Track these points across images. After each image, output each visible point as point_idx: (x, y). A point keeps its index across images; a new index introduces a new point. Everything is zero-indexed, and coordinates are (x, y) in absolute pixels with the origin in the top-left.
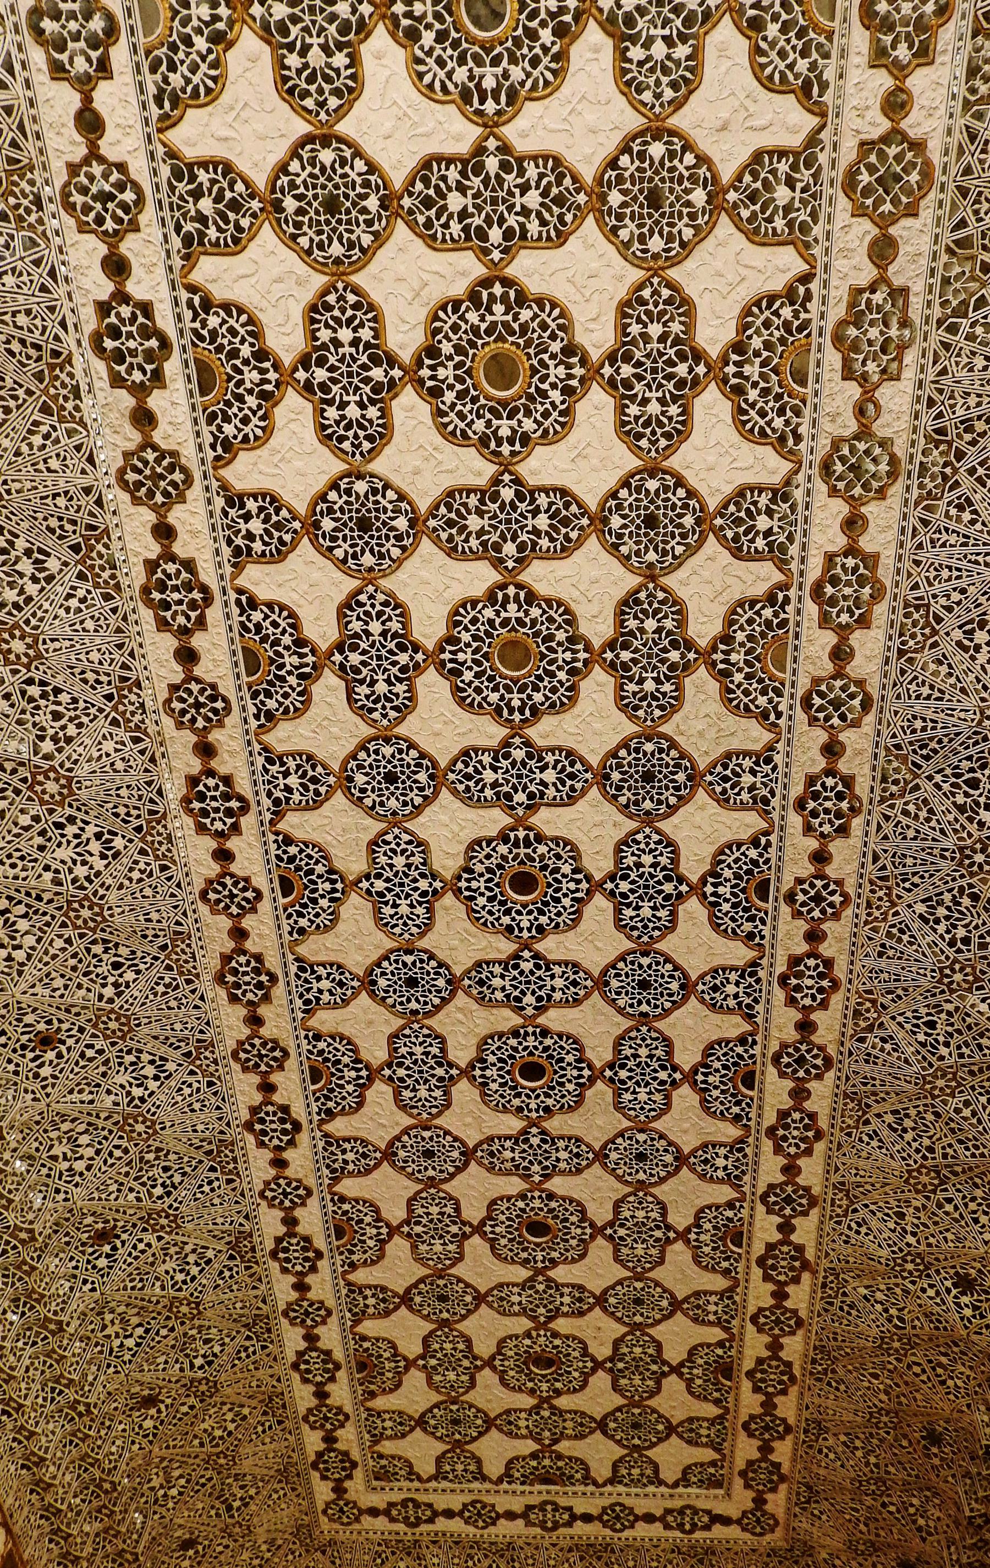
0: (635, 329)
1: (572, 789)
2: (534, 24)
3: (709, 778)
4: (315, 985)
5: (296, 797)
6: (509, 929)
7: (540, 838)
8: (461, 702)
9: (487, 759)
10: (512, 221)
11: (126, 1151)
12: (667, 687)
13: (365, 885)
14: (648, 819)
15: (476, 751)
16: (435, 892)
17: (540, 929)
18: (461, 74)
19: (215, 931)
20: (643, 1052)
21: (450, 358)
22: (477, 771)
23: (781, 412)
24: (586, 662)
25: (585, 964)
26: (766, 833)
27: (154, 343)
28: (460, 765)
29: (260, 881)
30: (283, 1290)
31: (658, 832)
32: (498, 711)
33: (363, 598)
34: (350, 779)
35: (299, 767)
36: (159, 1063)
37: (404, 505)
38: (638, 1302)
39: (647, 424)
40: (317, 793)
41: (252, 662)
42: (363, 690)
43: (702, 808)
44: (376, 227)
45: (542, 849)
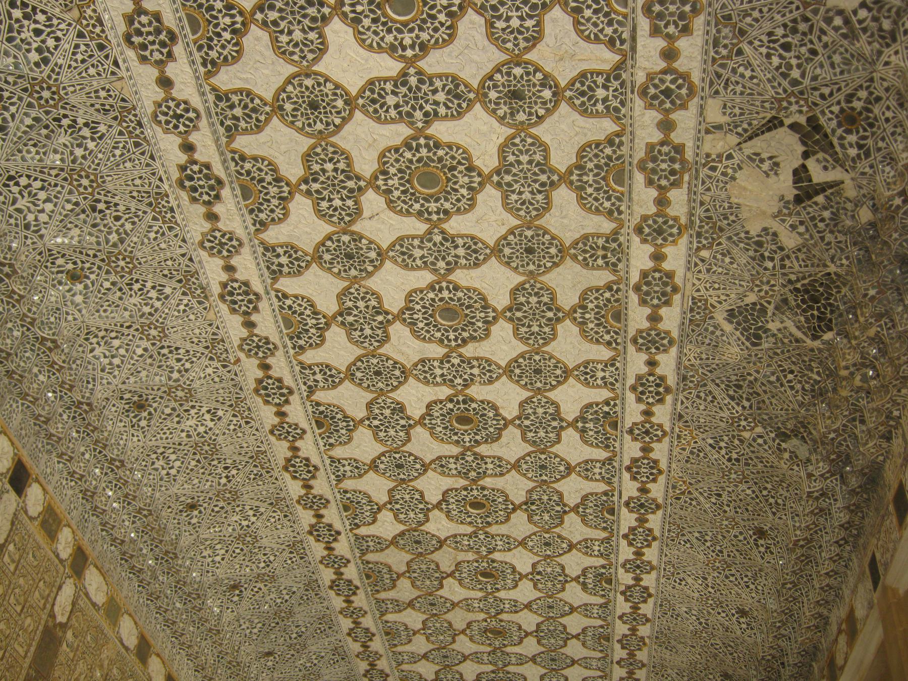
0: (511, 158)
2: (434, 12)
5: (321, 384)
9: (436, 364)
10: (428, 108)
11: (242, 550)
12: (547, 329)
16: (410, 425)
17: (476, 441)
18: (389, 38)
19: (280, 450)
20: (545, 498)
21: (395, 175)
23: (609, 199)
24: (494, 318)
26: (613, 399)
27: (212, 182)
28: (419, 367)
29: (304, 425)
30: (338, 603)
31: (546, 397)
34: (353, 375)
36: (256, 510)
37: (372, 246)
38: (552, 609)
39: (523, 203)
40: (333, 382)
41: (288, 323)
44: (343, 114)
45: (474, 405)
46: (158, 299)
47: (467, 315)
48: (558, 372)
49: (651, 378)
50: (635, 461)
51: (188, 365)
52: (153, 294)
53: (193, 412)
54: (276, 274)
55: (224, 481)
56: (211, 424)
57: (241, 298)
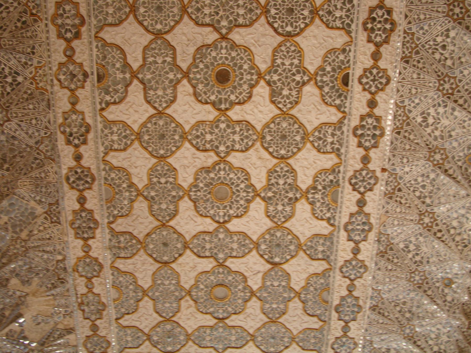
1: (197, 130)
3: (133, 137)
4: (344, 14)
5: (330, 131)
6: (232, 49)
7: (213, 104)
8: (247, 174)
9: (237, 147)
12: (155, 180)
13: (306, 78)
14: (160, 114)
15: (242, 151)
22: (242, 140)
24: (190, 191)
25: (192, 24)
26: (102, 109)
31: (155, 108)
32: (230, 169)
33: (283, 220)
35: (325, 146)
42: (289, 181)
43: (135, 121)
45: (213, 98)
46: (411, 242)
47: (209, 193)
48: (146, 137)
49: (76, 141)
50: (77, 35)
51: (420, 179)
52: (412, 247)
53: (437, 133)
54: (329, 238)
55: (452, 34)
56: (432, 111)
57: (359, 226)
